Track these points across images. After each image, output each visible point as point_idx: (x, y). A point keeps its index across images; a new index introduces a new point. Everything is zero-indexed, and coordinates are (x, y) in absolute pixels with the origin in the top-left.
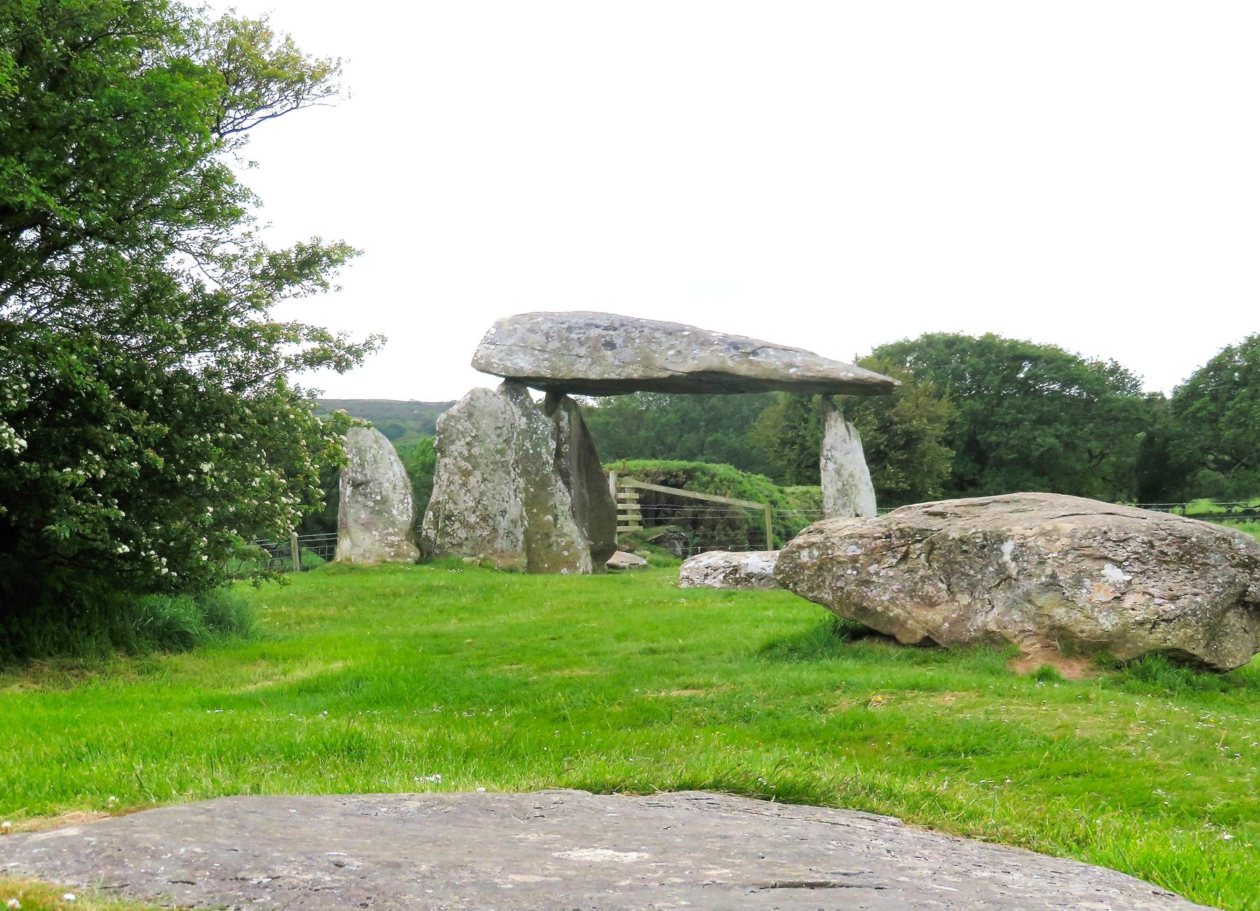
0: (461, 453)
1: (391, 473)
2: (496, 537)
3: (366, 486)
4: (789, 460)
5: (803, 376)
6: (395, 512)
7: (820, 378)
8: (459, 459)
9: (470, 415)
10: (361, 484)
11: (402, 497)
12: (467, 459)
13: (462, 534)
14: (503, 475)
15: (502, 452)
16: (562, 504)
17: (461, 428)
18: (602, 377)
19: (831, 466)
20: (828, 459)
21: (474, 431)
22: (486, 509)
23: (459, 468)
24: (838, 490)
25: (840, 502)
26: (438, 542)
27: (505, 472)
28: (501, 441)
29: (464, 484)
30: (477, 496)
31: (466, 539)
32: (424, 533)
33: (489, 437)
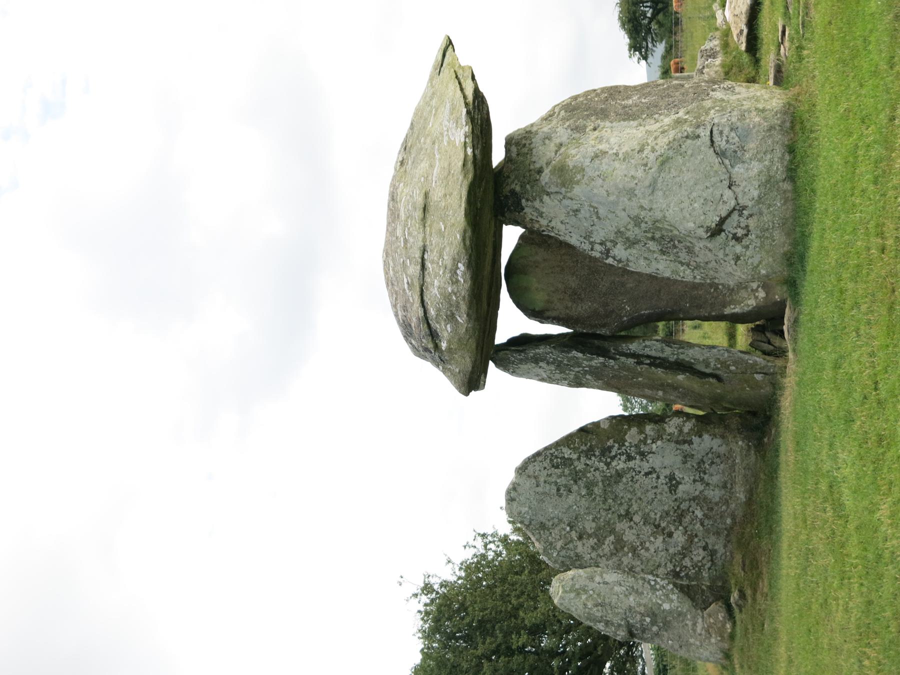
0: (593, 548)
1: (617, 589)
2: (705, 499)
3: (633, 626)
6: (666, 606)
8: (600, 552)
9: (543, 526)
11: (646, 585)
12: (600, 542)
13: (698, 554)
14: (621, 486)
15: (590, 486)
16: (662, 351)
17: (559, 544)
19: (619, 251)
20: (607, 253)
21: (563, 525)
22: (667, 513)
23: (612, 554)
24: (663, 252)
25: (683, 256)
27: (617, 482)
28: (575, 488)
29: (634, 550)
30: (648, 529)
31: (705, 548)
33: (571, 507)
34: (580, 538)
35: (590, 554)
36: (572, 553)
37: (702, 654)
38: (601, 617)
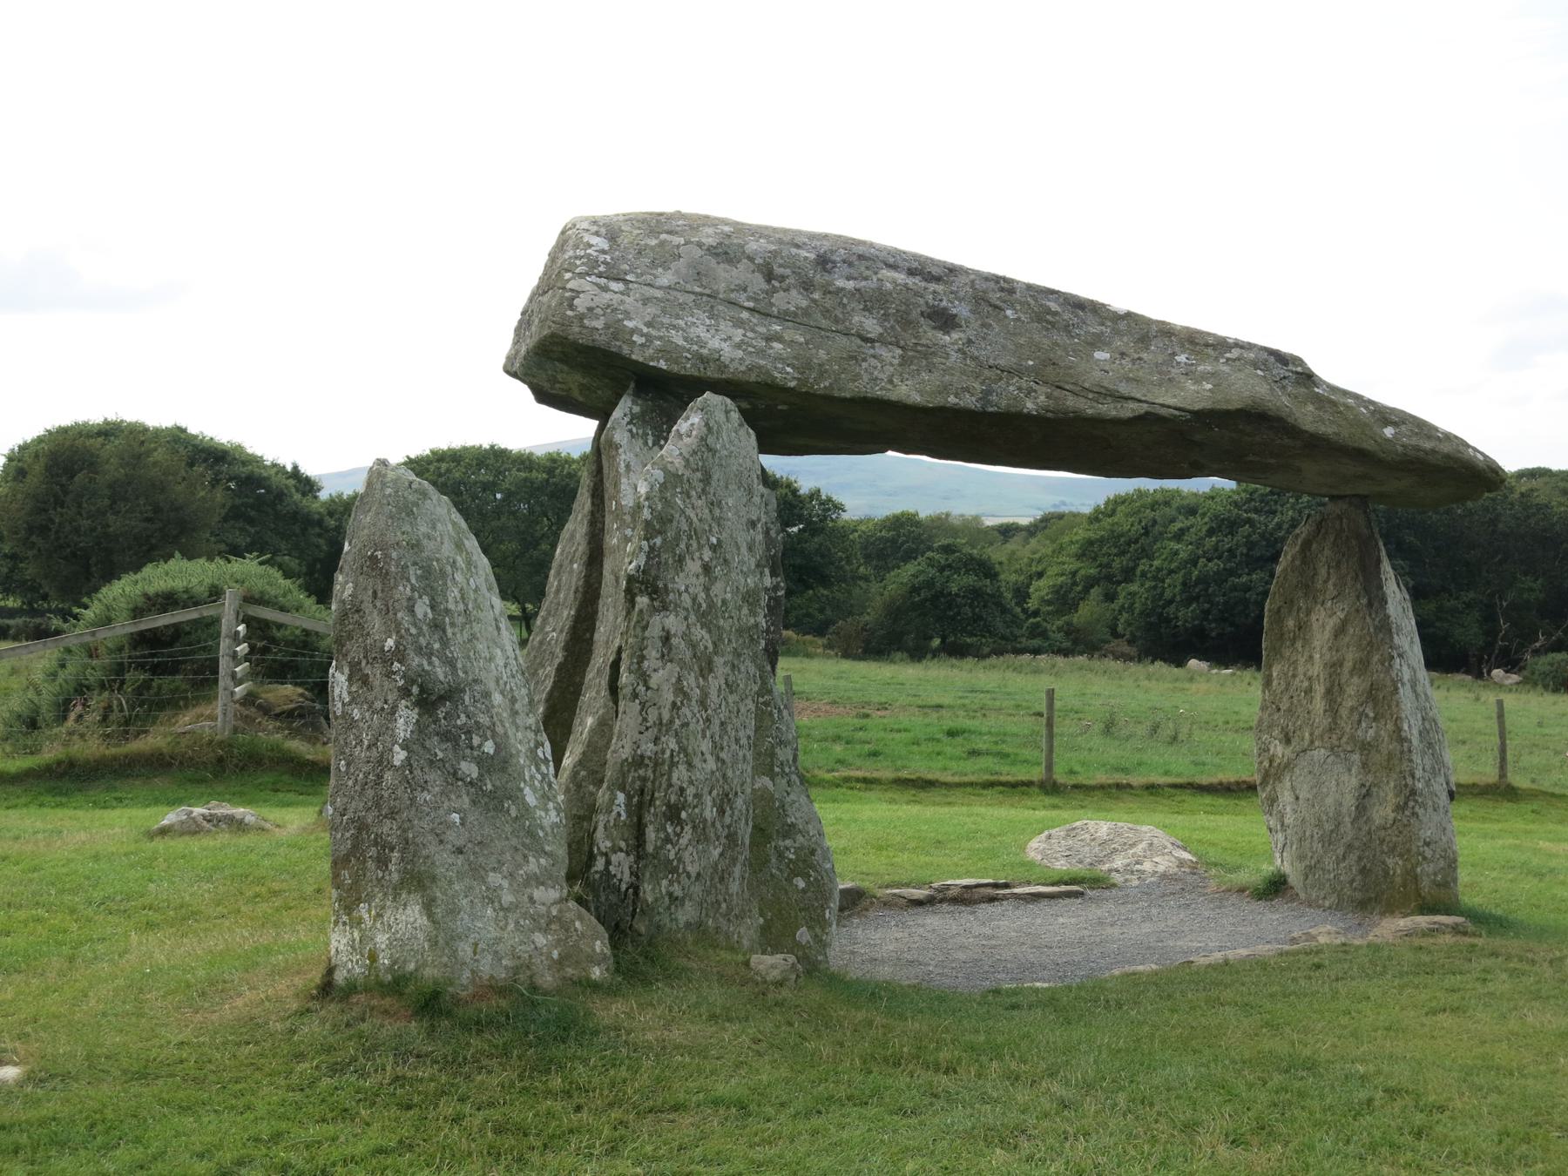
4: (39, 550)
5: (1417, 448)
6: (531, 799)
7: (1448, 456)
10: (442, 698)
18: (938, 401)
26: (648, 892)
32: (600, 864)
34: (707, 569)
35: (686, 590)
36: (683, 546)
37: (473, 917)
38: (447, 611)
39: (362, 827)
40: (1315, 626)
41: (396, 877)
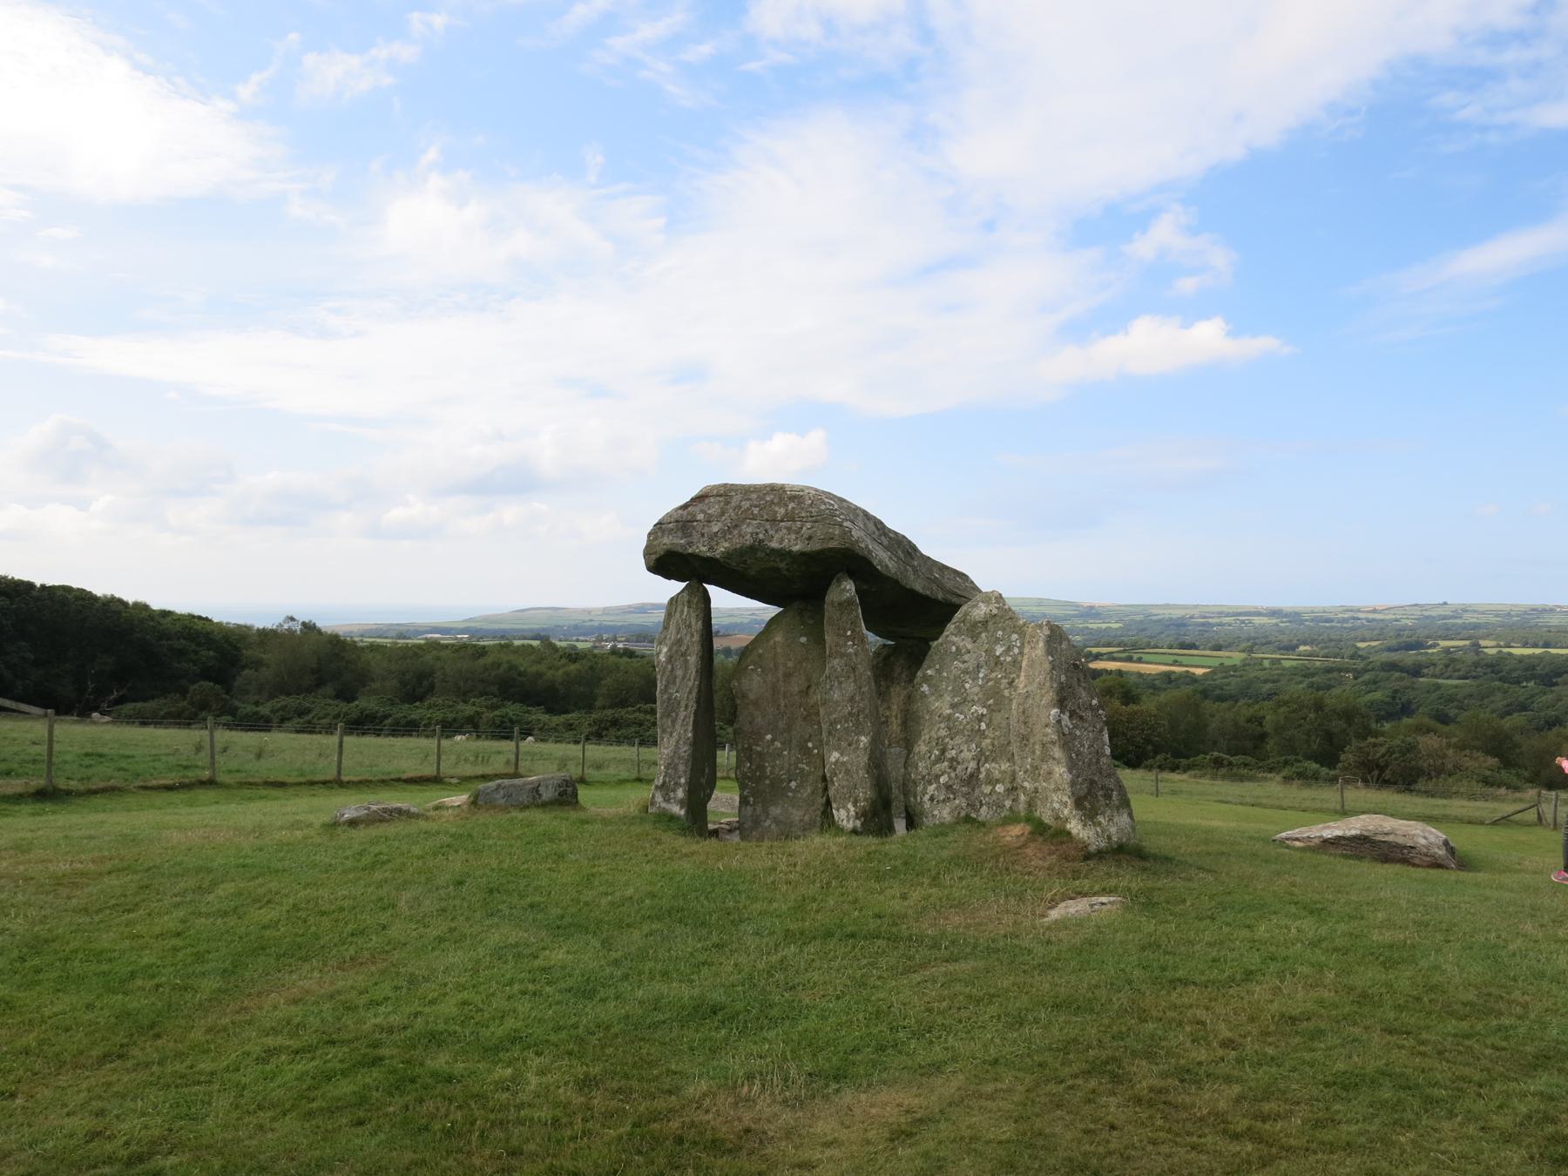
39: (1092, 782)
40: (893, 694)
41: (1117, 802)
